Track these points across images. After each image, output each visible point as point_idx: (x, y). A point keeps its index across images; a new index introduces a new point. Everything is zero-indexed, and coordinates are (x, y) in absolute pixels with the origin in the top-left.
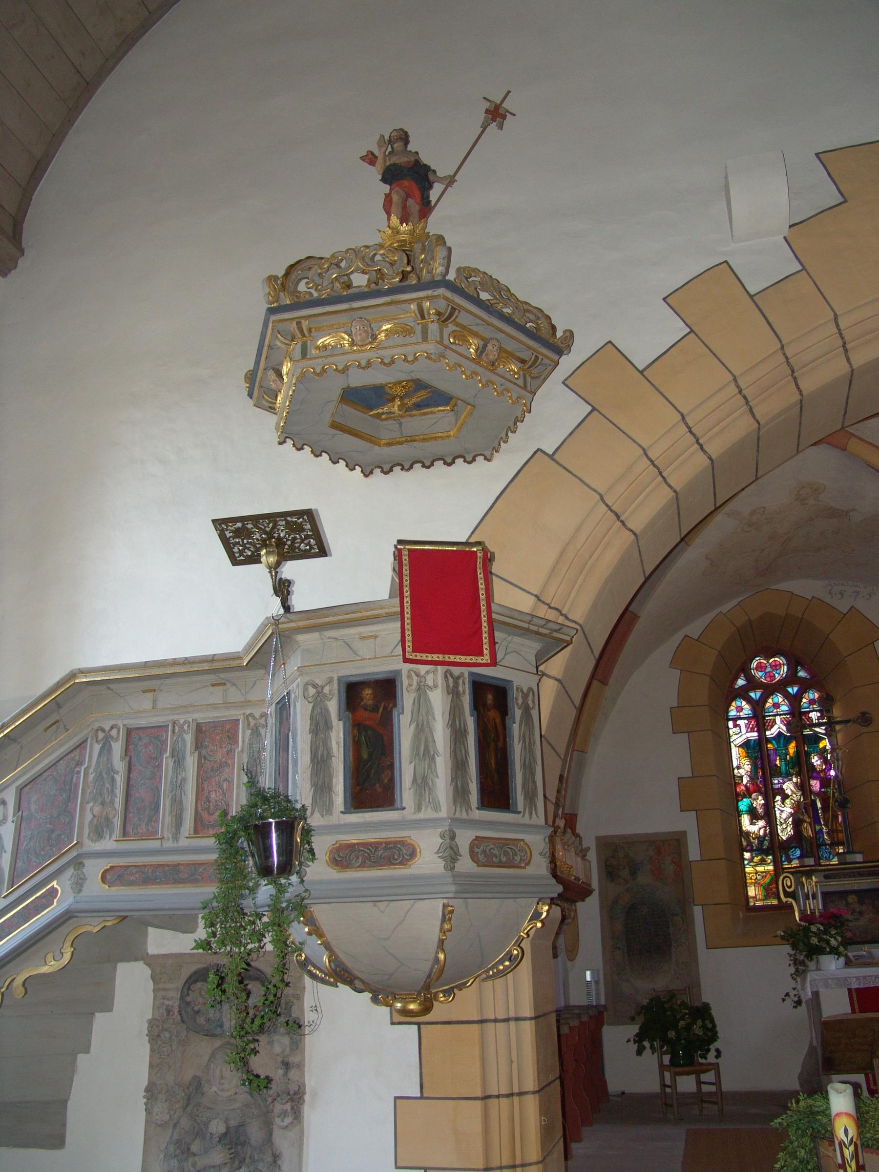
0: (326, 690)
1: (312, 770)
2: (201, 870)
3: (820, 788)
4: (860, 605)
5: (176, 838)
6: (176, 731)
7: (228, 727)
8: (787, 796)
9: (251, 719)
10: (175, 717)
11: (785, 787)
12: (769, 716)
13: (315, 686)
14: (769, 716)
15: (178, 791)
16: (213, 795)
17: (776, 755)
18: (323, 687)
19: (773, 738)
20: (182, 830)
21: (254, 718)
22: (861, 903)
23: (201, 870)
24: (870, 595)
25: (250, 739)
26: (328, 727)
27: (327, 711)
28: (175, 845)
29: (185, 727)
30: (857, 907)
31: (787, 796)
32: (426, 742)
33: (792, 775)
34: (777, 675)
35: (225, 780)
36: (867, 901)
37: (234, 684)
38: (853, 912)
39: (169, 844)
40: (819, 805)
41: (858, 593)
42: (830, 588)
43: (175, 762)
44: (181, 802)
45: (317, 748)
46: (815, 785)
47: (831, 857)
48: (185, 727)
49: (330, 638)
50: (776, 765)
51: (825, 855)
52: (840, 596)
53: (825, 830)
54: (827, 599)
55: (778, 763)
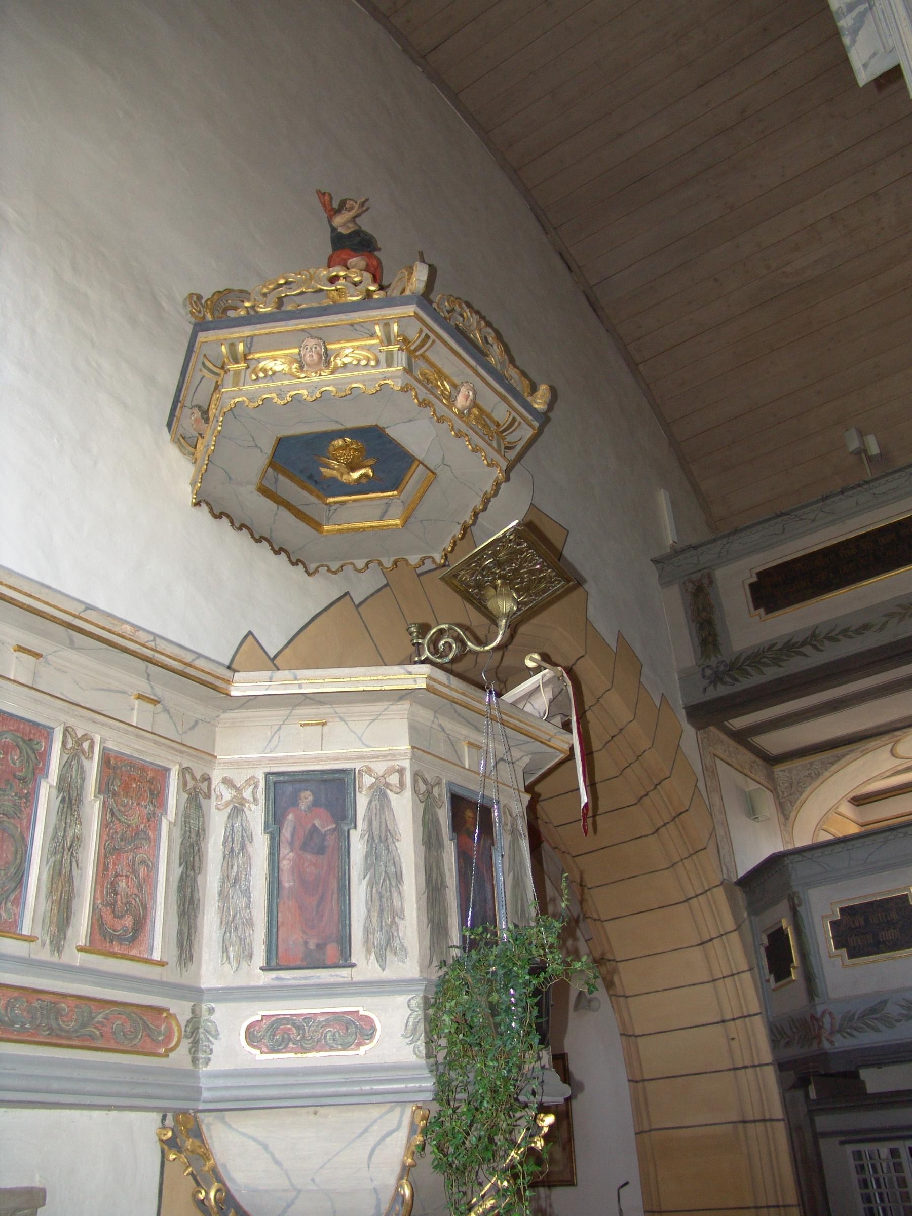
0: (436, 791)
1: (428, 898)
2: (99, 1018)
5: (57, 943)
6: (70, 746)
7: (150, 774)
9: (188, 777)
10: (71, 722)
13: (425, 782)
15: (67, 856)
16: (122, 884)
18: (432, 787)
20: (69, 933)
21: (194, 778)
23: (99, 1018)
25: (186, 808)
26: (440, 845)
27: (438, 821)
28: (55, 959)
29: (86, 745)
32: (522, 900)
35: (143, 862)
37: (166, 710)
39: (45, 954)
43: (63, 800)
44: (70, 878)
45: (431, 869)
48: (86, 745)
49: (440, 725)
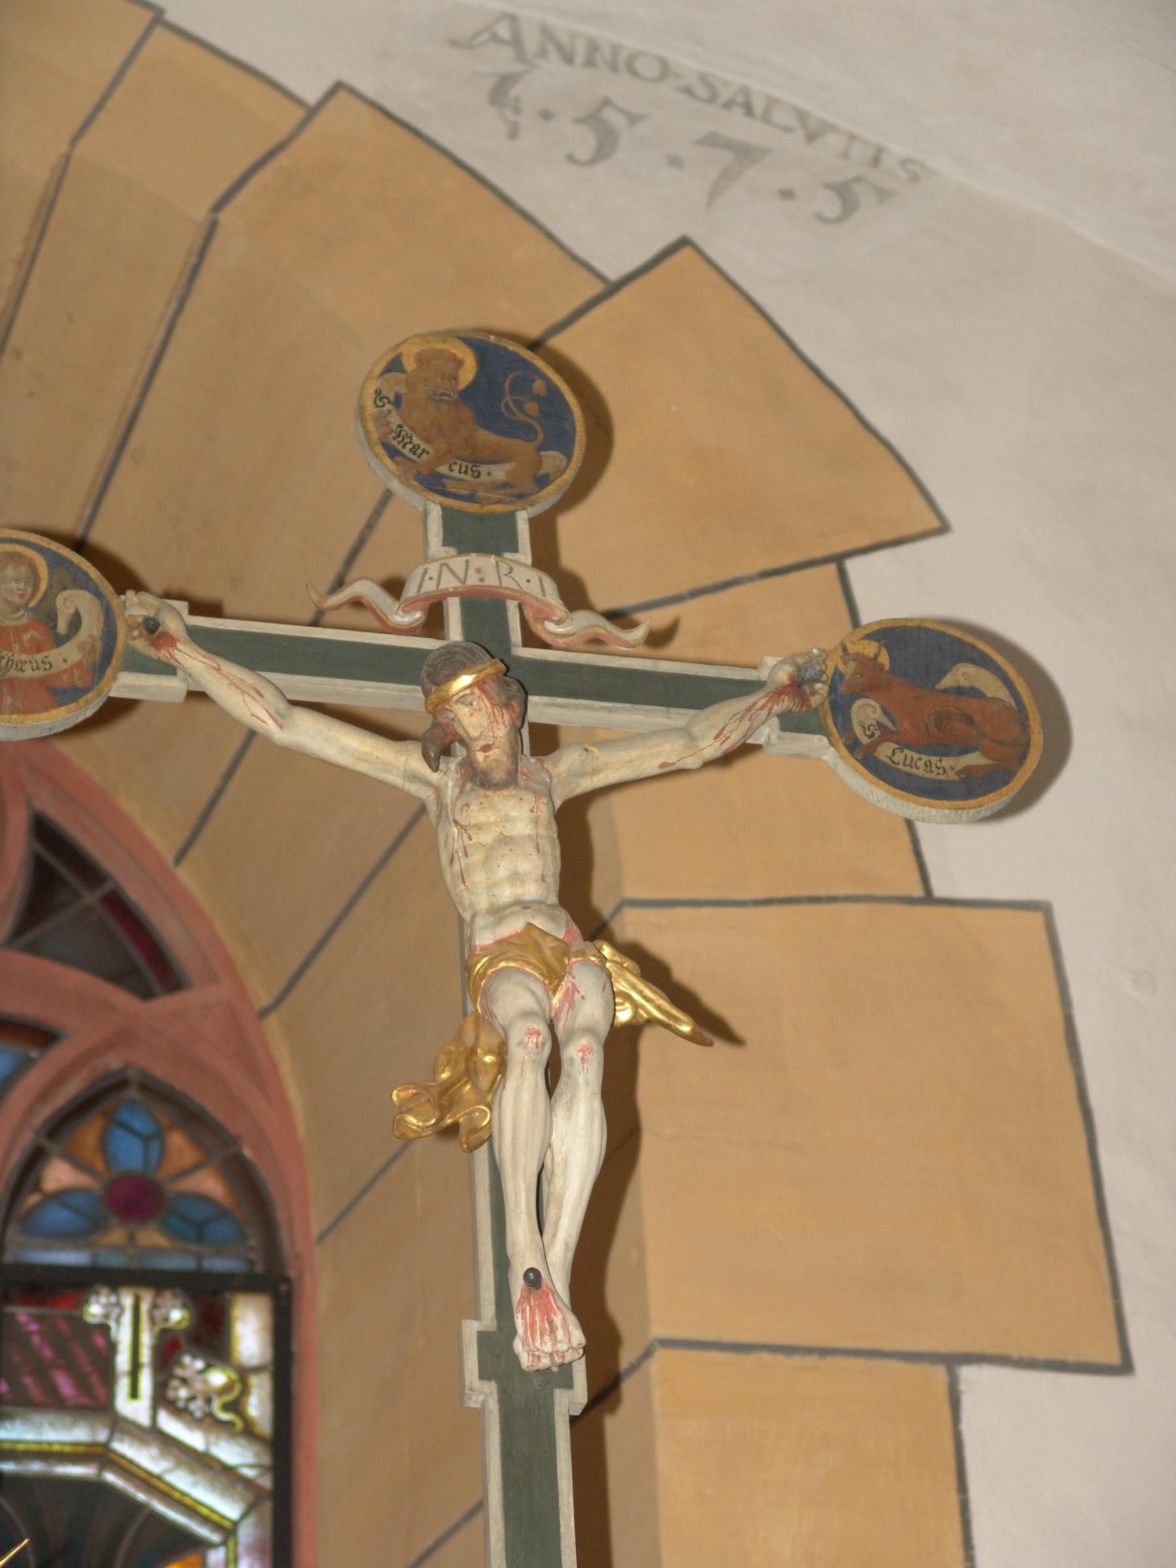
4: (758, 245)
24: (845, 192)
41: (746, 154)
42: (503, 60)
52: (584, 142)
54: (474, 136)
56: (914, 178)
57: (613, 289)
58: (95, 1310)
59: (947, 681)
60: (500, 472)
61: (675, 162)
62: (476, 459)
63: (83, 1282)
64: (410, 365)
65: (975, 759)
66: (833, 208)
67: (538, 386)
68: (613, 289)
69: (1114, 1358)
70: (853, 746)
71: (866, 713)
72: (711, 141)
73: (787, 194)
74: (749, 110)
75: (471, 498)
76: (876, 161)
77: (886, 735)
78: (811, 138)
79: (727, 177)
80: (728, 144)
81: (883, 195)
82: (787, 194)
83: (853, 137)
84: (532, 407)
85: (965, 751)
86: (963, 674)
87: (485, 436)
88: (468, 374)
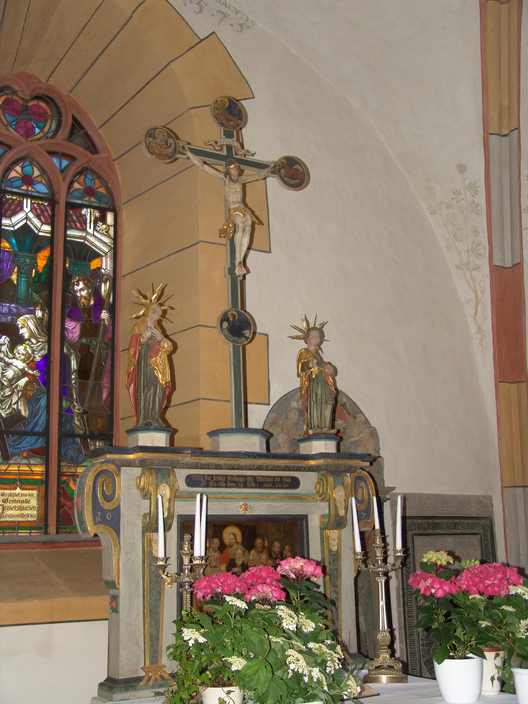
3: (81, 336)
4: (227, 35)
8: (21, 340)
11: (20, 322)
12: (13, 193)
14: (13, 193)
17: (14, 263)
19: (15, 233)
22: (248, 544)
24: (241, 25)
30: (239, 554)
31: (21, 340)
33: (35, 305)
34: (37, 131)
36: (259, 541)
38: (231, 564)
40: (74, 365)
41: (225, 15)
46: (74, 328)
47: (81, 458)
50: (11, 281)
51: (71, 453)
53: (77, 409)
55: (14, 277)
56: (253, 25)
57: (202, 41)
58: (83, 212)
59: (294, 167)
60: (232, 123)
61: (213, 15)
62: (229, 120)
63: (82, 206)
64: (219, 102)
65: (297, 181)
66: (239, 30)
67: (238, 108)
68: (202, 41)
69: (269, 251)
70: (281, 177)
71: (283, 172)
72: (219, 11)
73: (232, 25)
74: (226, 6)
75: (228, 128)
76: (247, 20)
77: (285, 176)
78: (236, 13)
79: (221, 20)
80: (222, 13)
81: (248, 28)
82: (232, 25)
83: (244, 14)
84: (237, 112)
85: (296, 180)
86: (296, 166)
87: (230, 117)
88: (227, 105)
